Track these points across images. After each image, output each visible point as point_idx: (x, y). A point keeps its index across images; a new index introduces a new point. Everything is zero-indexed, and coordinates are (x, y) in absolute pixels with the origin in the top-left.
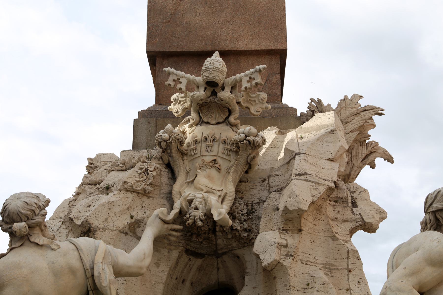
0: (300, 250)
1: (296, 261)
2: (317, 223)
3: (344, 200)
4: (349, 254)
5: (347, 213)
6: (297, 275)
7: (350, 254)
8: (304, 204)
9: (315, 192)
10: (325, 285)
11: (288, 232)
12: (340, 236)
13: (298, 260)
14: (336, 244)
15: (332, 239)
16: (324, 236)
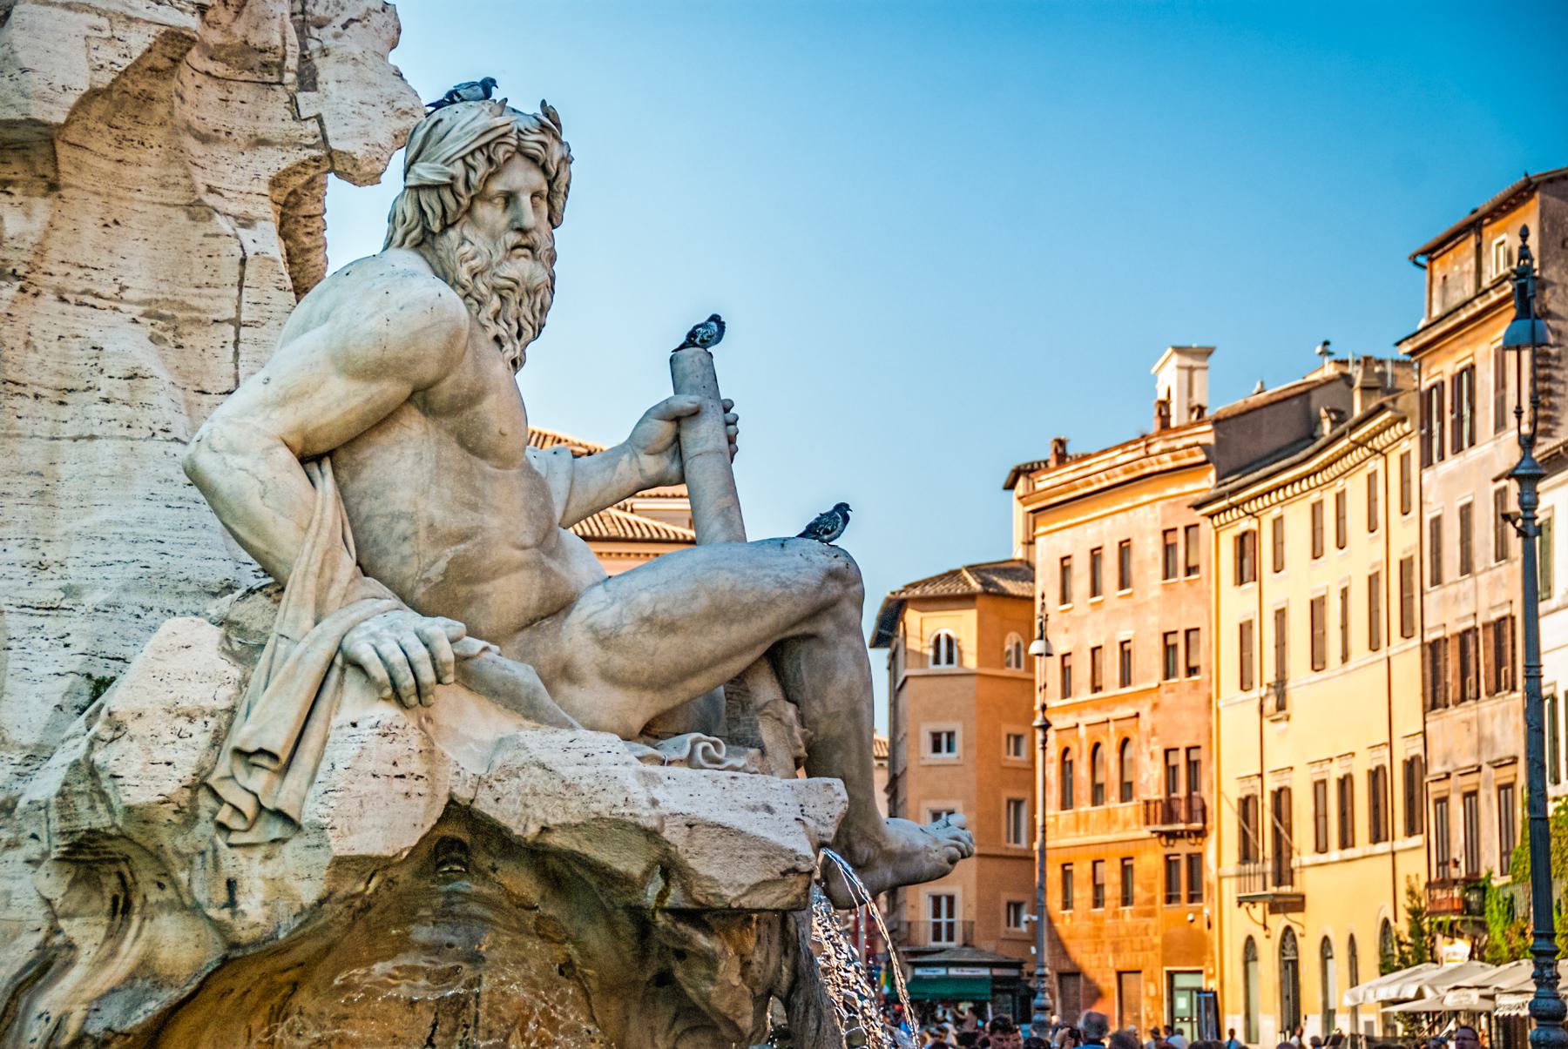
0: (54, 255)
1: (36, 295)
2: (130, 154)
3: (269, 57)
4: (247, 272)
5: (273, 115)
6: (39, 344)
7: (250, 272)
8: (51, 102)
9: (108, 54)
10: (135, 382)
11: (9, 189)
12: (229, 200)
13: (44, 291)
14: (202, 232)
15: (189, 212)
16: (162, 204)
